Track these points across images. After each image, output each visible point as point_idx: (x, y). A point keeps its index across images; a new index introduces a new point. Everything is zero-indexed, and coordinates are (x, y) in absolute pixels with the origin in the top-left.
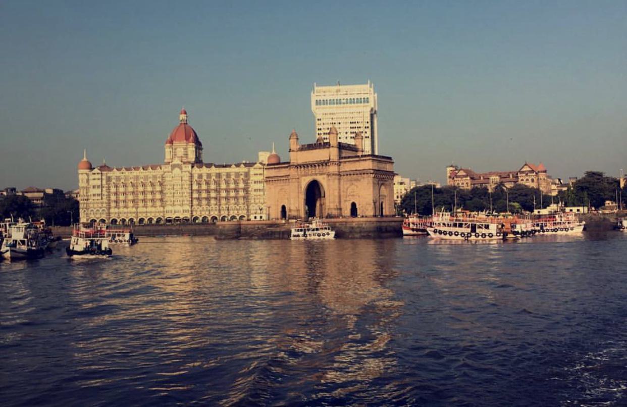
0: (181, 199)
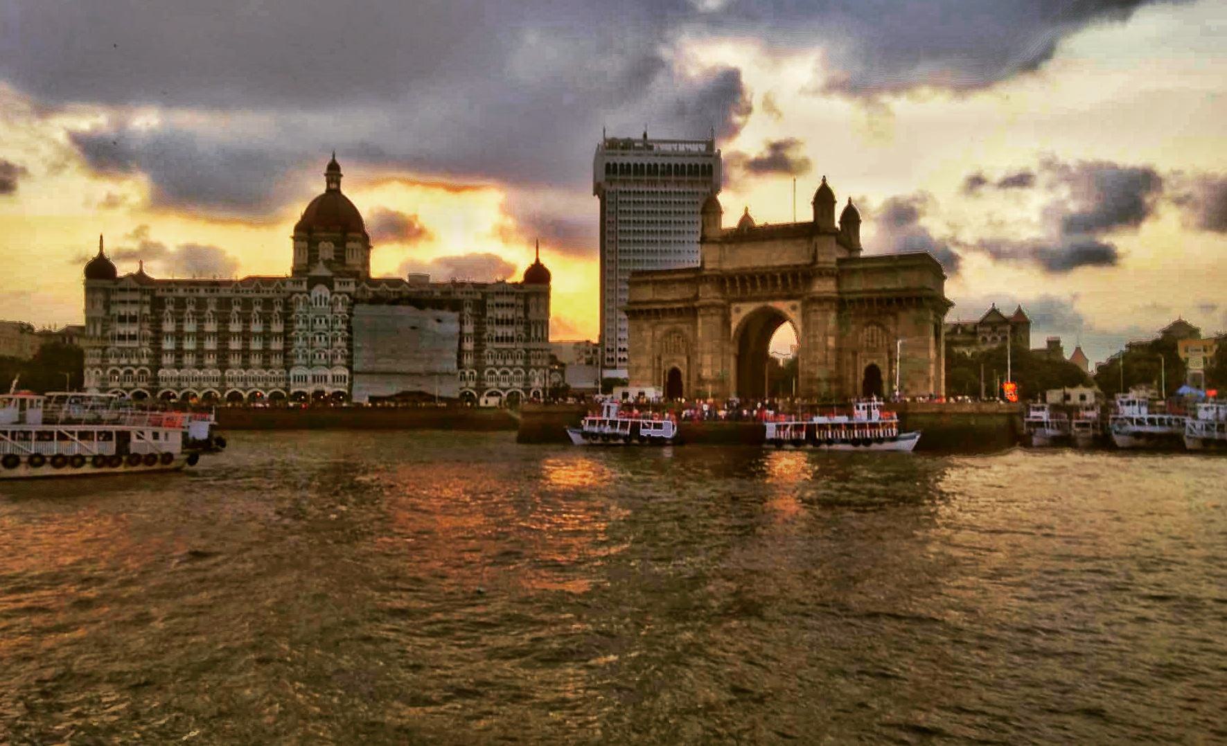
0: (329, 352)
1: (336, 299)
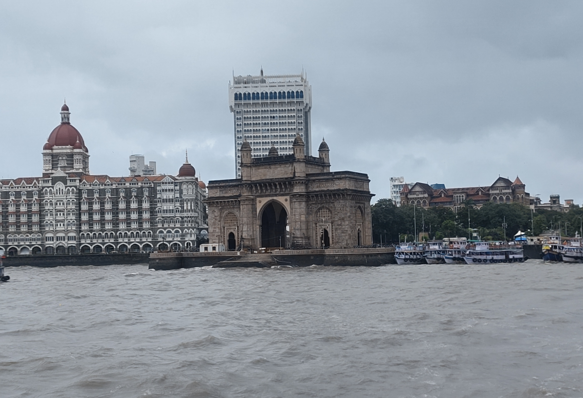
1: (69, 189)
